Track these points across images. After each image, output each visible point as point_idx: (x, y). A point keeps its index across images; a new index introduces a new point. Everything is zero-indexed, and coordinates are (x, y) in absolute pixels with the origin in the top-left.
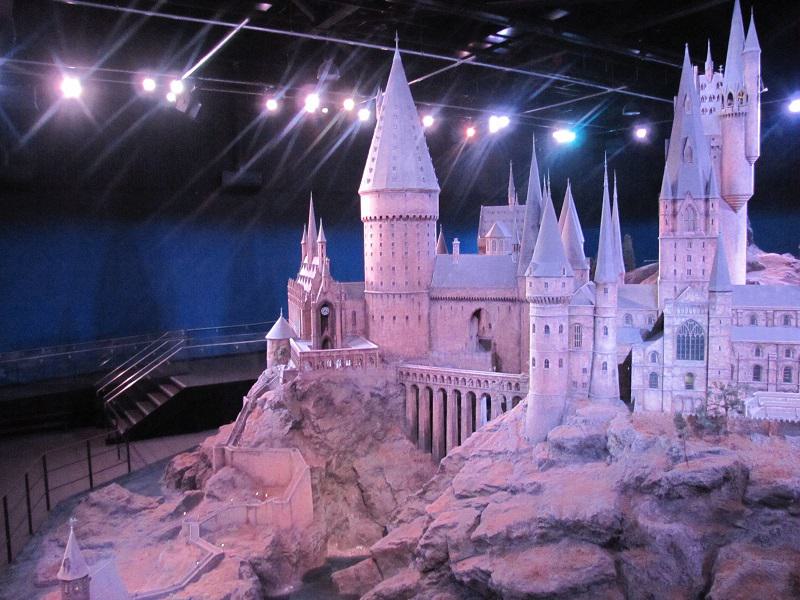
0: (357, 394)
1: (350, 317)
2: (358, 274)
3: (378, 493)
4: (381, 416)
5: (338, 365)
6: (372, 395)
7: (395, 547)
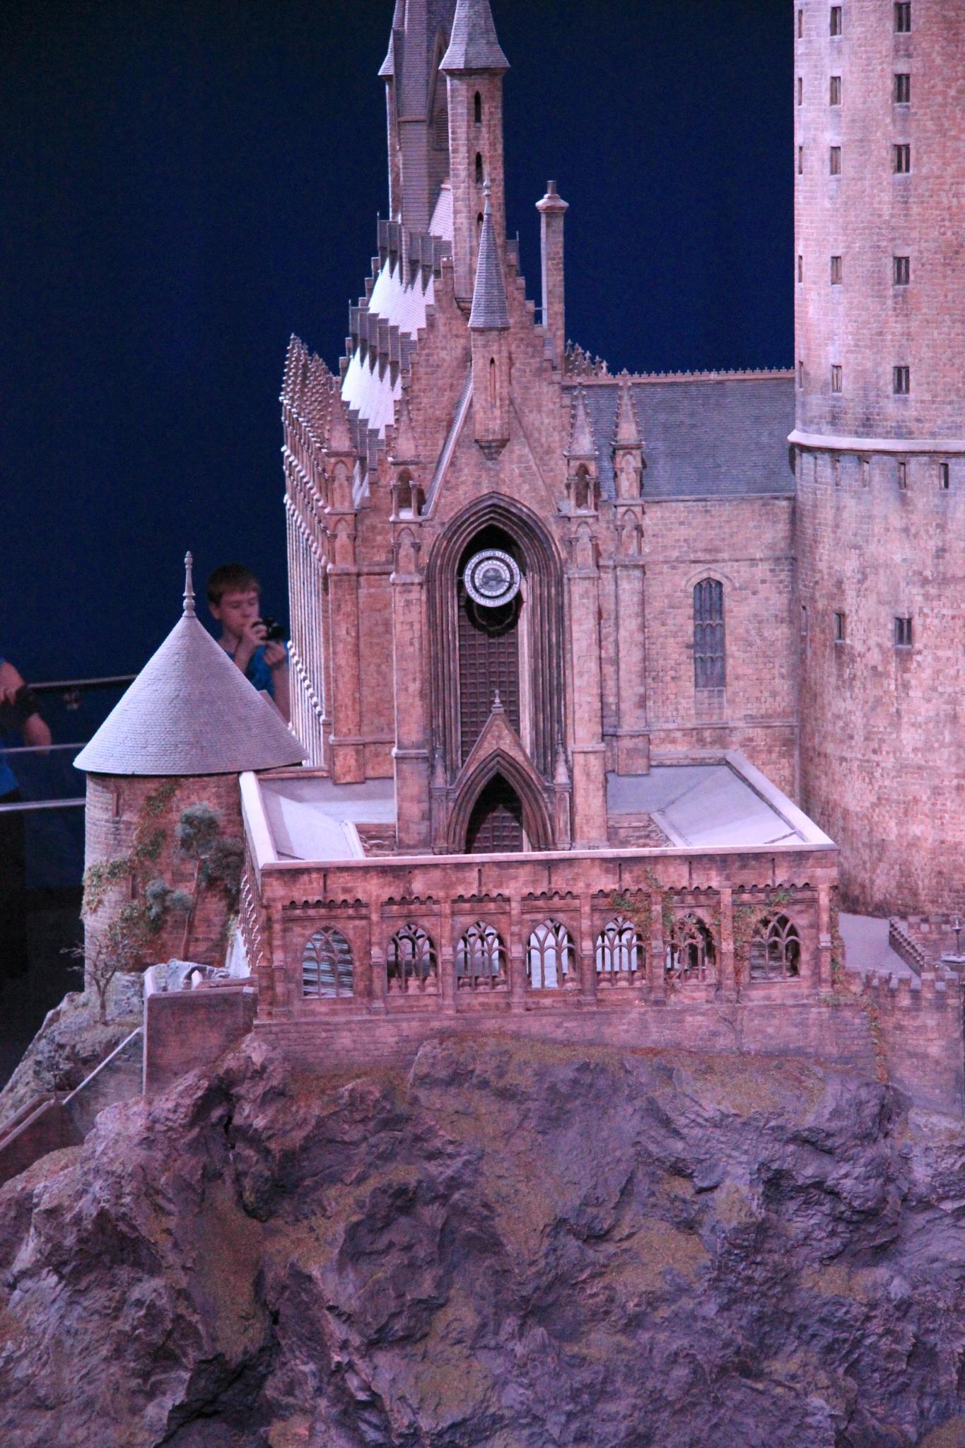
0: (677, 1174)
1: (684, 622)
2: (753, 325)
4: (844, 1351)
5: (547, 968)
6: (775, 1184)
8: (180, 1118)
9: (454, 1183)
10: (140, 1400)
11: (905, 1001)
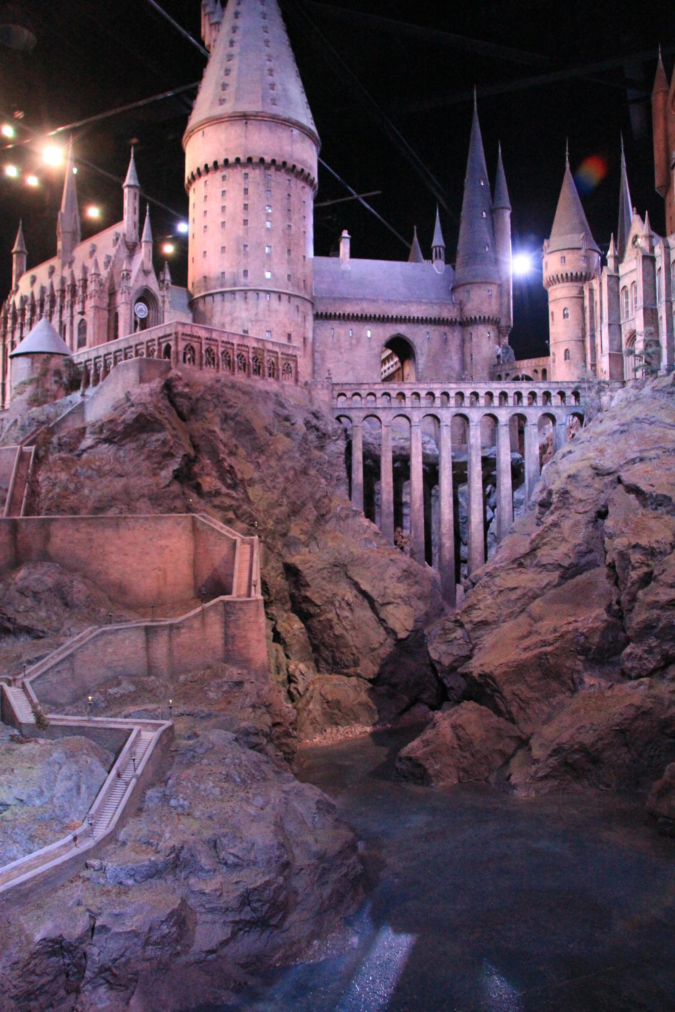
3: (346, 613)
7: (549, 649)
8: (158, 390)
9: (236, 415)
10: (158, 471)
11: (320, 387)
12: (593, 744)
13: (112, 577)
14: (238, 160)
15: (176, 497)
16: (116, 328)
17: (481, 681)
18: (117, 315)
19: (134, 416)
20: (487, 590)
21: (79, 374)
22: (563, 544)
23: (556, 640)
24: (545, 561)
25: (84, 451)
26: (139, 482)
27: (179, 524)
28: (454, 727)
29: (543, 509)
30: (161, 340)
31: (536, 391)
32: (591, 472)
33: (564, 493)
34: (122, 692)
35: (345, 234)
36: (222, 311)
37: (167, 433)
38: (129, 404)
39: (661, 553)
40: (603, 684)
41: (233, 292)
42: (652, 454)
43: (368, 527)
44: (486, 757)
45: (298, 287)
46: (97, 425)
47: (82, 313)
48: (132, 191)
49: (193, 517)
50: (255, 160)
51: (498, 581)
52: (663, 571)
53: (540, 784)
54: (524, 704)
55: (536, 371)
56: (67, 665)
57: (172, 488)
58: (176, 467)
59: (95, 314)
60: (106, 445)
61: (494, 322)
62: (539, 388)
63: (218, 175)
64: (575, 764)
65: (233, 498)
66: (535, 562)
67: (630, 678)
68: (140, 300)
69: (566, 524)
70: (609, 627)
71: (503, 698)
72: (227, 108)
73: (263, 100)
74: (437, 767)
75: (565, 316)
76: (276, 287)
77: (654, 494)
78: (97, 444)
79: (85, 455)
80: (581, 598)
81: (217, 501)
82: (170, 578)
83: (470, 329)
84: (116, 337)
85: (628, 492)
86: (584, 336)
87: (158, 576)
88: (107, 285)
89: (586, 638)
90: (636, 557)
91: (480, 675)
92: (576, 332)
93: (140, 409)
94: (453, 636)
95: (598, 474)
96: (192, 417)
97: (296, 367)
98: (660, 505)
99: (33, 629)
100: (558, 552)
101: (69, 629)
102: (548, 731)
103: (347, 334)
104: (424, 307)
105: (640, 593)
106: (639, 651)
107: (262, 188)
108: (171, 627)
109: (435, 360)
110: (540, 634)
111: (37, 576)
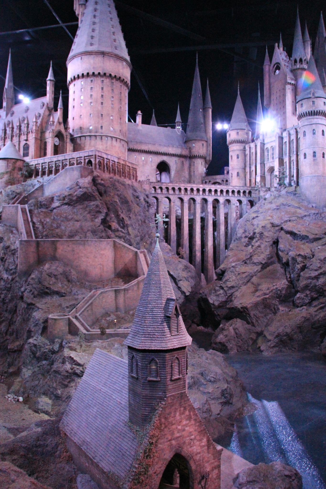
7: (267, 296)
10: (94, 219)
12: (291, 333)
13: (82, 268)
14: (99, 73)
15: (102, 231)
16: (45, 149)
17: (242, 310)
18: (45, 143)
19: (82, 193)
20: (233, 273)
21: (32, 170)
22: (262, 254)
23: (270, 293)
24: (256, 261)
25: (54, 208)
26: (86, 224)
27: (108, 244)
28: (234, 329)
29: (250, 240)
30: (86, 158)
31: (235, 190)
32: (270, 225)
33: (261, 234)
34: (111, 319)
35: (139, 112)
36: (90, 144)
37: (98, 201)
38: (78, 187)
39: (309, 258)
40: (287, 310)
41: (96, 136)
42: (294, 218)
43: (167, 247)
44: (246, 341)
45: (124, 136)
46: (61, 197)
47: (27, 140)
48: (52, 82)
49: (114, 241)
50: (108, 75)
51: (237, 269)
52: (311, 265)
53: (271, 350)
54: (258, 318)
55: (223, 181)
56: (90, 307)
57: (100, 227)
58: (103, 217)
59: (35, 141)
60: (67, 206)
61: (203, 158)
62: (225, 188)
63: (89, 80)
64: (284, 341)
65: (123, 232)
66: (251, 262)
67: (298, 307)
68: (57, 136)
69: (262, 246)
70: (289, 287)
71: (250, 317)
72: (94, 48)
73: (112, 47)
74: (231, 346)
75: (238, 158)
76: (115, 135)
77: (301, 235)
78: (61, 205)
79: (55, 211)
80: (273, 276)
81: (117, 234)
82: (105, 269)
83: (193, 160)
84: (45, 154)
85: (286, 234)
86: (245, 166)
87: (100, 268)
88: (40, 128)
89: (281, 291)
90: (299, 259)
91: (242, 308)
92: (241, 165)
93: (85, 190)
94: (219, 293)
95: (273, 226)
96: (105, 195)
97: (136, 173)
98: (303, 239)
99: (60, 292)
100: (261, 258)
101: (77, 292)
102: (272, 328)
103: (142, 158)
104: (174, 149)
105: (302, 273)
106: (302, 296)
107: (110, 89)
108: (125, 290)
109: (178, 172)
110: (262, 290)
111: (54, 268)
